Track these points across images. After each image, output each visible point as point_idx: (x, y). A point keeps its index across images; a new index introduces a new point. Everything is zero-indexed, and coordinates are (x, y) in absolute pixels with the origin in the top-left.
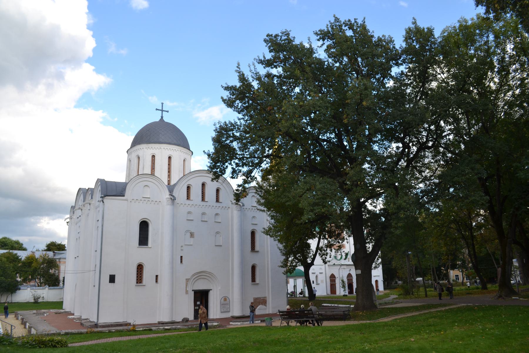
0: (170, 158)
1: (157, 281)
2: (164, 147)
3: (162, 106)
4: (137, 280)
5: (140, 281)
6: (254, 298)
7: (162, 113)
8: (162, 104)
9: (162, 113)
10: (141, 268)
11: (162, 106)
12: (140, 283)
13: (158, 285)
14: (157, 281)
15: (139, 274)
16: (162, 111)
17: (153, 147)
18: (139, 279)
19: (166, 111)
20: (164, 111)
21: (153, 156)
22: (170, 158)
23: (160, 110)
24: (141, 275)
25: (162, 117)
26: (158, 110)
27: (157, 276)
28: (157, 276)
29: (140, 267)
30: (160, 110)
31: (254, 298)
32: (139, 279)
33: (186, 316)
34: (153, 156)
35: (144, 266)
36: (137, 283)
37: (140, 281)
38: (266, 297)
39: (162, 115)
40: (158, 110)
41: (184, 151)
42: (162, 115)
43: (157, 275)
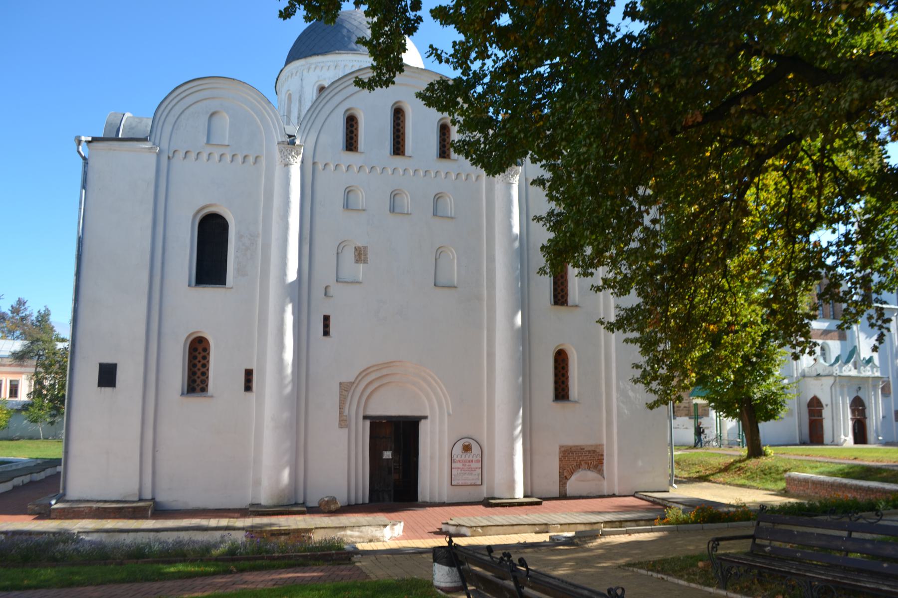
1: (248, 387)
6: (561, 447)
13: (252, 396)
14: (248, 387)
24: (204, 370)
27: (249, 373)
28: (249, 373)
31: (561, 447)
37: (202, 386)
43: (249, 367)
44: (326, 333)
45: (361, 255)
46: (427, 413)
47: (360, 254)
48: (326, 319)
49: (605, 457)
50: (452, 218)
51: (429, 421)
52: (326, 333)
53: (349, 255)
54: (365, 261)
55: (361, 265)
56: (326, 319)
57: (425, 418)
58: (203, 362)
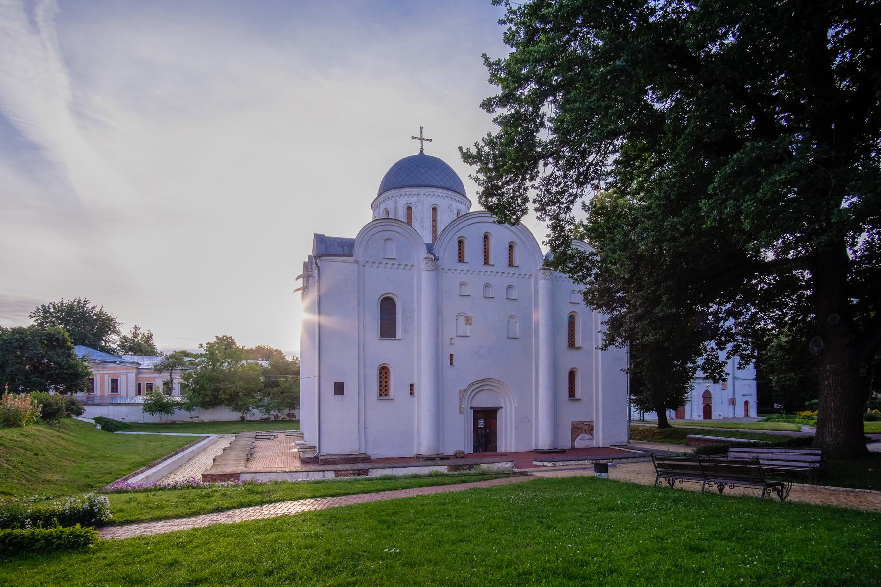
0: (434, 209)
1: (411, 394)
2: (425, 192)
4: (381, 390)
5: (385, 393)
10: (386, 373)
12: (386, 395)
13: (415, 399)
14: (411, 394)
15: (383, 382)
18: (384, 390)
20: (424, 140)
21: (409, 209)
22: (434, 209)
23: (419, 139)
27: (412, 385)
28: (412, 385)
29: (385, 371)
30: (419, 139)
32: (384, 390)
34: (409, 209)
36: (381, 395)
37: (385, 393)
40: (415, 138)
41: (457, 199)
45: (468, 320)
46: (503, 405)
48: (451, 355)
49: (594, 427)
50: (516, 300)
51: (503, 410)
52: (451, 364)
53: (462, 320)
54: (471, 324)
55: (469, 327)
56: (451, 355)
57: (502, 408)
58: (385, 380)
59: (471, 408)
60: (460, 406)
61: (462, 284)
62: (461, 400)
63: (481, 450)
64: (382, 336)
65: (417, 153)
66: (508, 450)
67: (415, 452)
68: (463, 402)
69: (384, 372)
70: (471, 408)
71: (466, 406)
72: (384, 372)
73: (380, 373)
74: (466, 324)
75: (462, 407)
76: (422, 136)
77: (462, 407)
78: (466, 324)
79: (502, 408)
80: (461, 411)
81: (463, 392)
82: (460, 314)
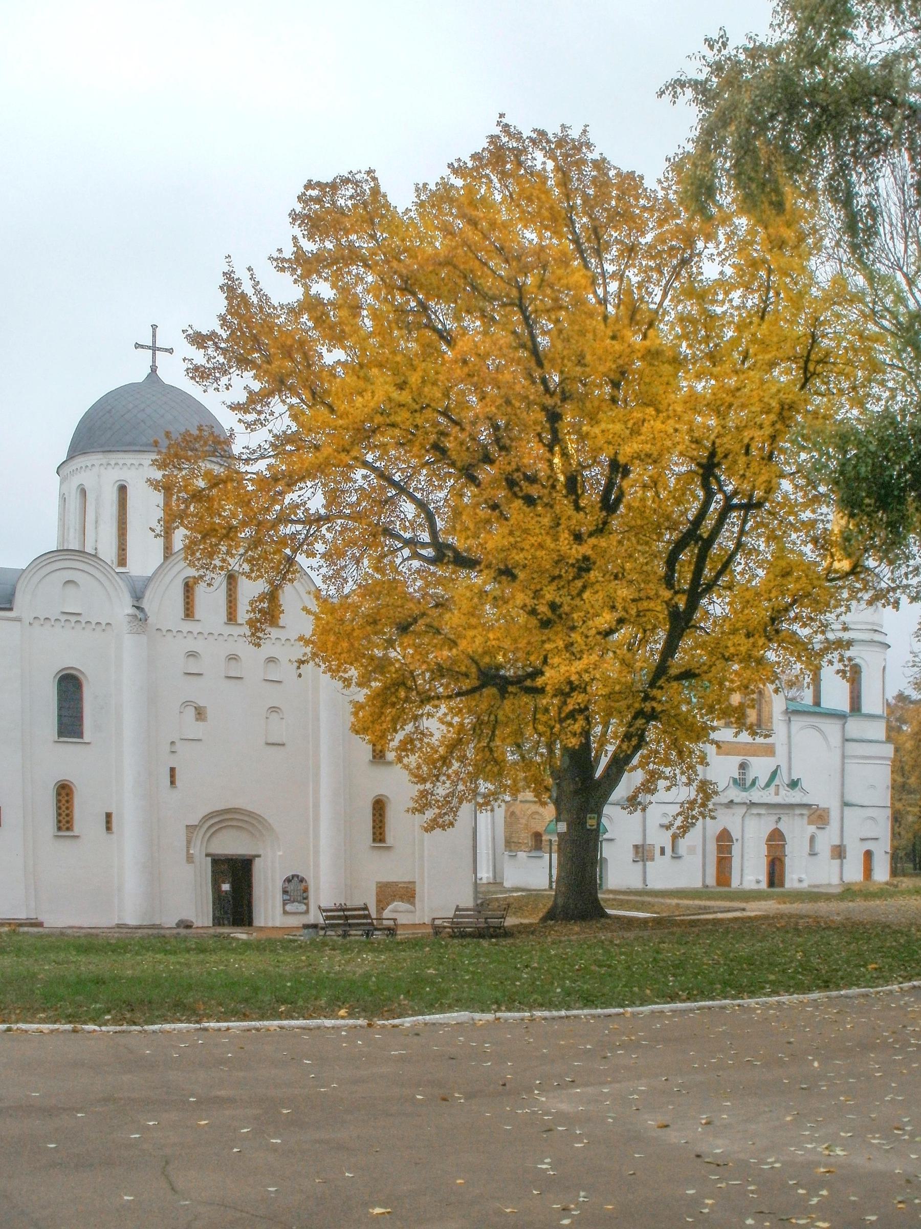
1: (109, 828)
3: (154, 336)
4: (59, 822)
7: (154, 355)
8: (154, 327)
9: (154, 355)
11: (154, 336)
14: (109, 828)
15: (64, 808)
16: (154, 349)
17: (121, 462)
19: (166, 350)
20: (159, 349)
23: (149, 348)
25: (154, 369)
26: (142, 347)
27: (109, 816)
28: (109, 816)
30: (149, 348)
33: (189, 914)
35: (74, 789)
38: (414, 882)
39: (154, 361)
40: (142, 347)
42: (154, 361)
44: (173, 782)
45: (200, 714)
46: (261, 852)
47: (199, 714)
48: (172, 770)
52: (173, 782)
53: (191, 712)
55: (200, 723)
56: (172, 770)
57: (259, 856)
59: (207, 855)
60: (188, 851)
61: (192, 655)
62: (189, 842)
63: (226, 922)
64: (61, 733)
65: (139, 375)
66: (270, 925)
67: (116, 921)
68: (192, 845)
69: (64, 792)
70: (207, 855)
71: (197, 850)
72: (64, 792)
73: (58, 794)
74: (197, 720)
75: (191, 852)
76: (154, 342)
77: (191, 852)
78: (197, 720)
79: (259, 856)
80: (190, 859)
81: (190, 828)
82: (186, 703)
